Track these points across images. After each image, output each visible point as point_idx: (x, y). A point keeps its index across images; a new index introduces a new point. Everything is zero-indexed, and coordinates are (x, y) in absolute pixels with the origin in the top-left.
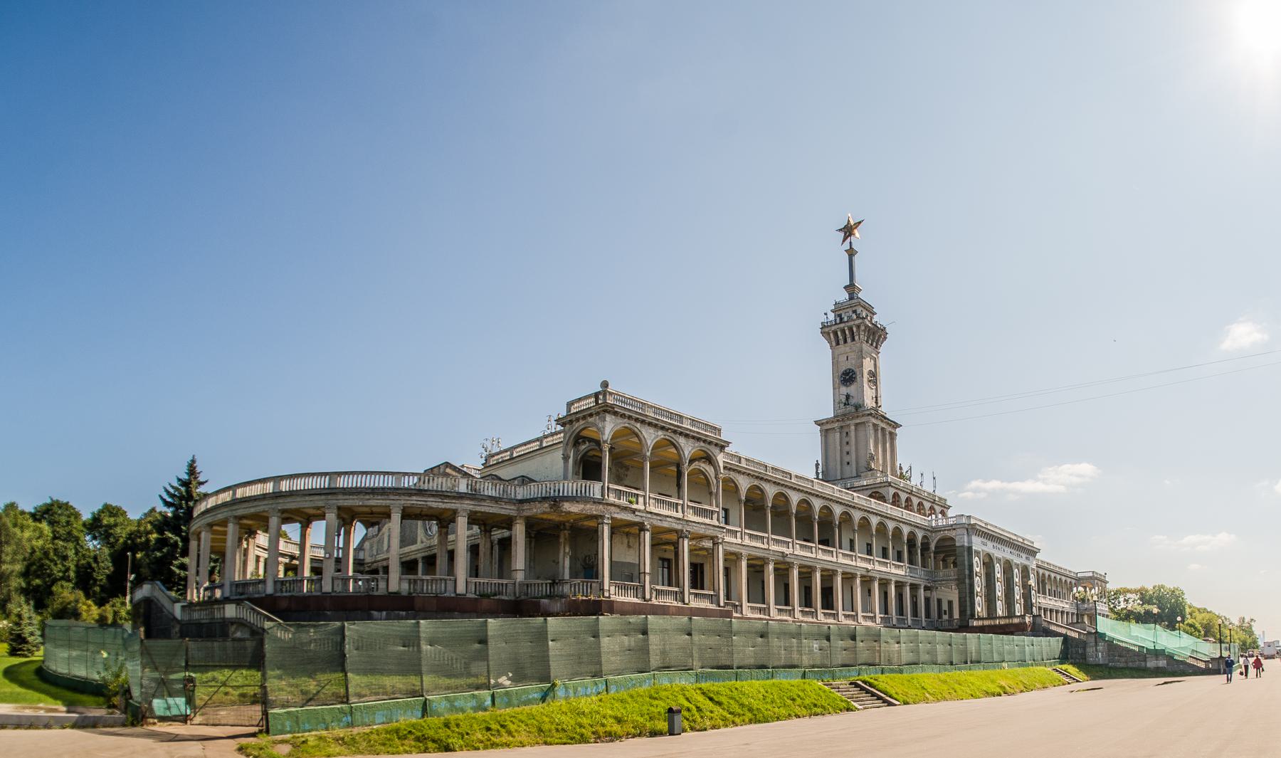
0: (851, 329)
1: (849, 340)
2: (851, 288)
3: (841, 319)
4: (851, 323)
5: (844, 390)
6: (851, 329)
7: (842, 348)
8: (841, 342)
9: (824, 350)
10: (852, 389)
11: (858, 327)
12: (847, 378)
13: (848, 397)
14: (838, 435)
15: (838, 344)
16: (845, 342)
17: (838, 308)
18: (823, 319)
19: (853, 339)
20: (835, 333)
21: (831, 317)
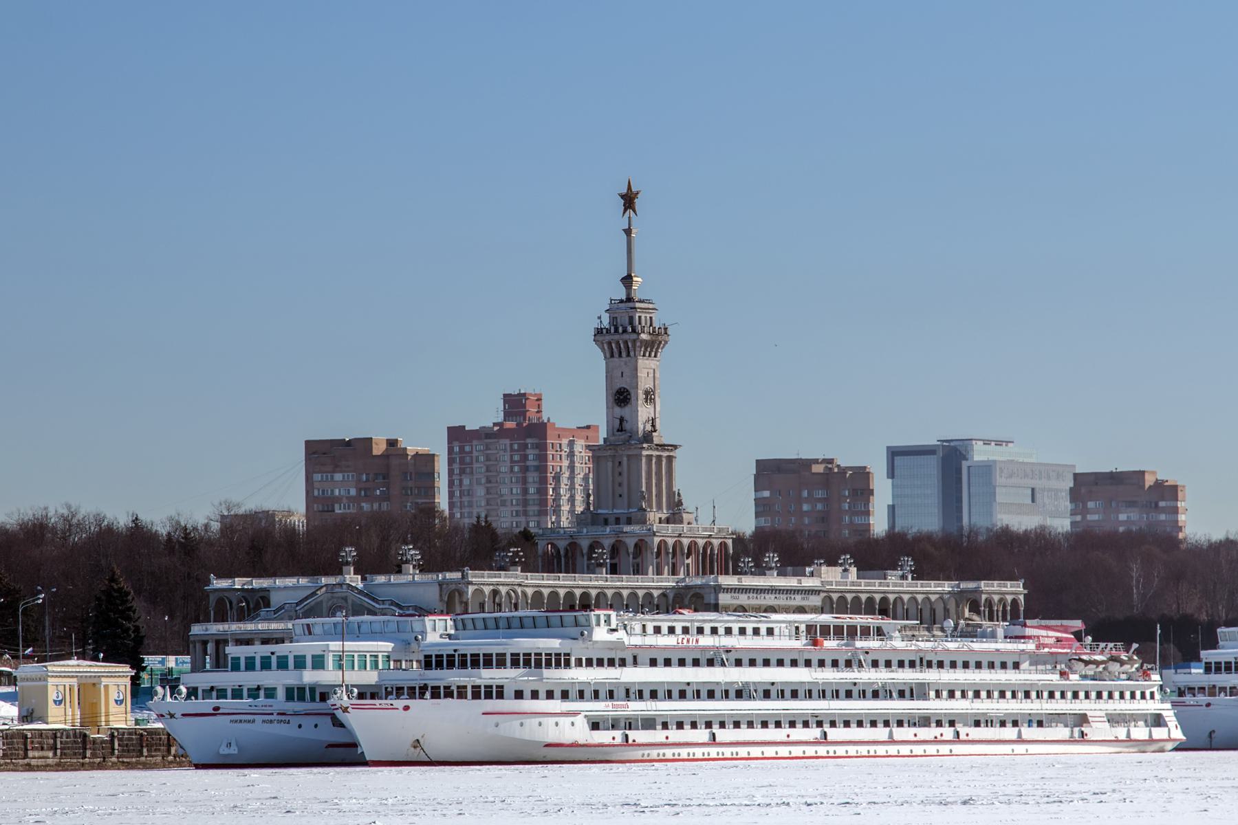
0: (626, 342)
1: (624, 354)
2: (627, 280)
3: (616, 330)
4: (626, 337)
5: (618, 411)
6: (626, 342)
7: (616, 359)
8: (616, 355)
9: (596, 360)
10: (626, 412)
11: (634, 341)
12: (621, 397)
13: (622, 420)
14: (610, 464)
15: (612, 356)
16: (620, 355)
17: (613, 309)
18: (596, 324)
19: (628, 355)
20: (610, 344)
21: (606, 322)
